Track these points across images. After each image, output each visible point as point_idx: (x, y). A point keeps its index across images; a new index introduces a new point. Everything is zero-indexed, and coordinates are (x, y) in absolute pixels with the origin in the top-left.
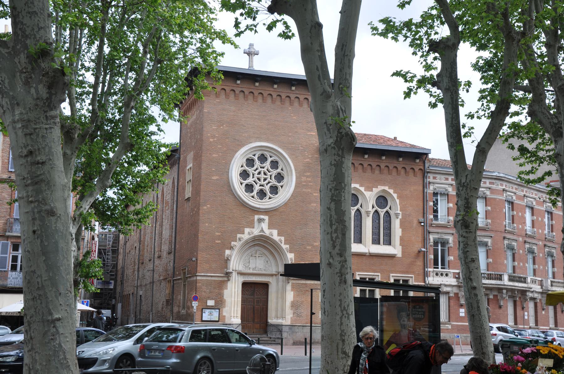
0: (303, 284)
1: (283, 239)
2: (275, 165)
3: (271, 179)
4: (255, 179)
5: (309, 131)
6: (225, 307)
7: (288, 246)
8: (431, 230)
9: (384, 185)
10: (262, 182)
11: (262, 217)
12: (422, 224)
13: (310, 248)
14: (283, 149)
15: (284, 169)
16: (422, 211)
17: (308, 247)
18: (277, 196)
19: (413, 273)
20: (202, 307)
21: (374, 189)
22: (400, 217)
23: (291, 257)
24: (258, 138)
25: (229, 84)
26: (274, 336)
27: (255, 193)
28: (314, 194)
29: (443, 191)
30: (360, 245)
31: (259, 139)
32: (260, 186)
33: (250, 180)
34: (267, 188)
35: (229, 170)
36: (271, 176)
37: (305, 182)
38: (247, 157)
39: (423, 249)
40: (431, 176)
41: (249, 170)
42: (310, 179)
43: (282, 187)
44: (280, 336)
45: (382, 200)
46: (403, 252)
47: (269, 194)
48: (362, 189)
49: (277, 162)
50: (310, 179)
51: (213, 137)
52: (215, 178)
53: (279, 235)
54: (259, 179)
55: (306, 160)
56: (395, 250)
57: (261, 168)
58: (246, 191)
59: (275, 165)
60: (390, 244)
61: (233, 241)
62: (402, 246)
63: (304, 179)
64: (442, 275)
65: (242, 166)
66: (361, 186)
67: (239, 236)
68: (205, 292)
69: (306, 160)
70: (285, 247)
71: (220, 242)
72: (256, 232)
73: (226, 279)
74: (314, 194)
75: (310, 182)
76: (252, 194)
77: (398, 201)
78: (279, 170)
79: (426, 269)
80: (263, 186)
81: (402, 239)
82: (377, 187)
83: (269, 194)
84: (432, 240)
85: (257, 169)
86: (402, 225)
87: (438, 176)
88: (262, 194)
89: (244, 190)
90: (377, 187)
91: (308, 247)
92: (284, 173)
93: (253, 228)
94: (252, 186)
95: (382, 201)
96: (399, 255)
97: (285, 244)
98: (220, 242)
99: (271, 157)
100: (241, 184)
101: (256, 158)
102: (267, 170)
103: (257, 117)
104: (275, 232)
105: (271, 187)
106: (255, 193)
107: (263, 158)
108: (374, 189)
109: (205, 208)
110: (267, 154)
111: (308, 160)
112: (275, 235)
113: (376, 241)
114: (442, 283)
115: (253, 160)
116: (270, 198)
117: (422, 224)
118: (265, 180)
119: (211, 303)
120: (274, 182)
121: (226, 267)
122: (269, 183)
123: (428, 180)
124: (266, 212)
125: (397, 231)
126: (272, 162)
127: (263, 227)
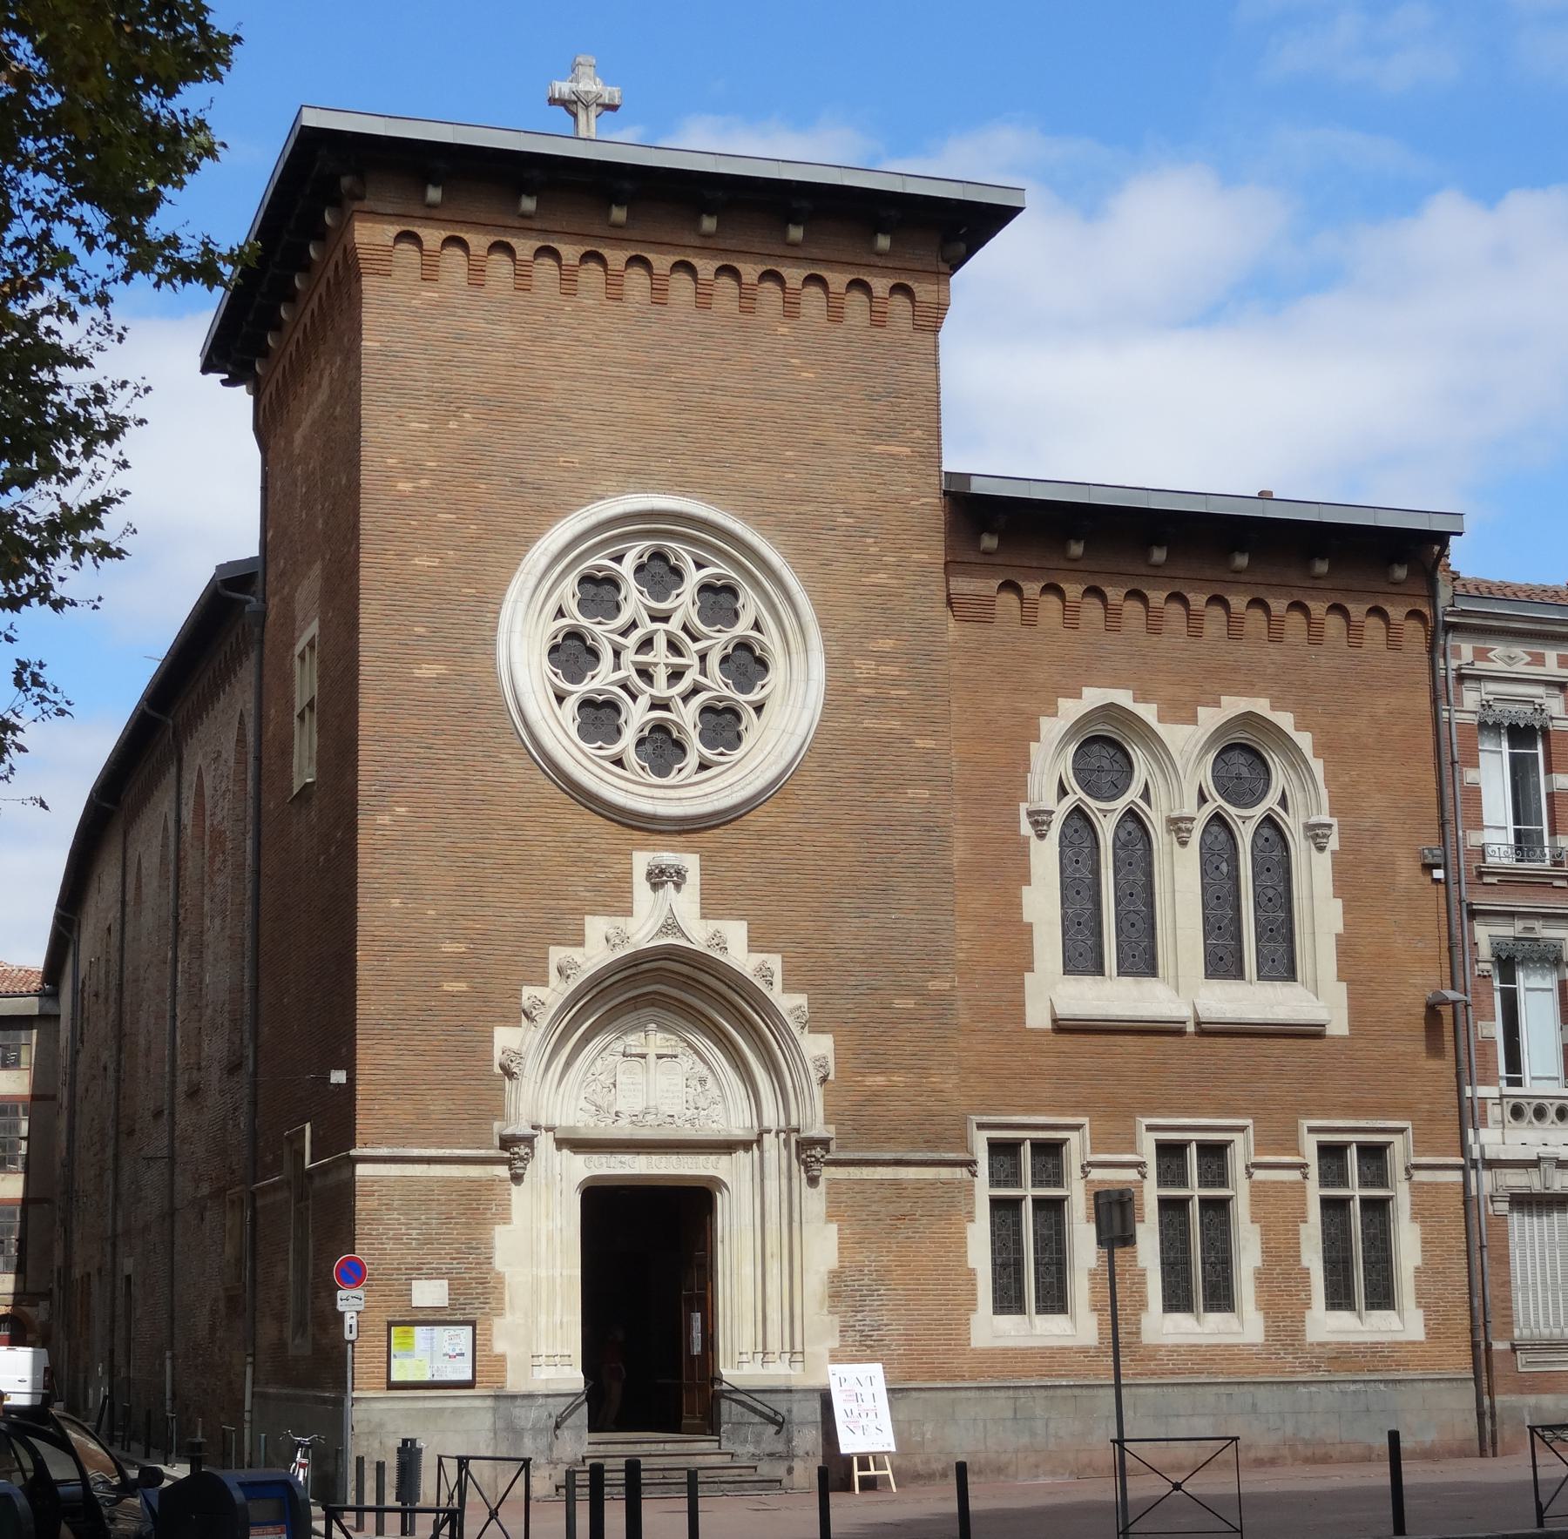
0: (881, 1183)
1: (775, 962)
2: (719, 599)
3: (703, 672)
5: (879, 437)
7: (801, 1000)
8: (1482, 901)
9: (1249, 690)
10: (661, 689)
11: (668, 858)
12: (1439, 874)
13: (910, 1003)
14: (759, 527)
15: (768, 622)
16: (1434, 811)
17: (899, 1003)
18: (737, 754)
19: (1405, 1110)
20: (385, 1317)
21: (1202, 712)
22: (1333, 843)
23: (817, 1052)
25: (483, 218)
26: (751, 1448)
27: (629, 738)
28: (919, 743)
29: (1522, 714)
30: (1147, 983)
31: (639, 479)
32: (653, 707)
33: (602, 679)
34: (687, 717)
35: (495, 629)
36: (703, 658)
37: (868, 683)
39: (1452, 995)
41: (598, 629)
43: (759, 709)
44: (780, 1447)
47: (696, 749)
48: (1147, 712)
49: (731, 591)
50: (894, 671)
51: (413, 470)
52: (427, 671)
54: (645, 673)
55: (874, 579)
56: (1316, 998)
57: (653, 619)
58: (586, 733)
59: (719, 599)
60: (1290, 974)
61: (531, 983)
62: (1350, 982)
63: (865, 668)
64: (1540, 1113)
65: (560, 613)
67: (557, 954)
69: (874, 579)
70: (788, 1003)
71: (462, 986)
73: (503, 1171)
74: (919, 743)
75: (896, 683)
76: (614, 750)
77: (1317, 766)
78: (742, 628)
79: (1468, 1091)
80: (666, 707)
81: (1346, 949)
82: (1217, 704)
83: (696, 749)
84: (1485, 951)
85: (634, 625)
86: (1345, 883)
87: (1499, 650)
88: (662, 746)
89: (573, 730)
90: (1217, 704)
91: (899, 1003)
92: (771, 641)
93: (629, 913)
94: (612, 706)
95: (1245, 772)
96: (1339, 1026)
97: (788, 988)
98: (462, 986)
99: (699, 566)
100: (560, 699)
101: (626, 569)
102: (685, 628)
103: (624, 372)
105: (706, 710)
106: (629, 738)
107: (660, 573)
108: (1202, 712)
109: (385, 819)
110: (683, 554)
111: (881, 578)
112: (733, 945)
113: (1222, 962)
114: (1544, 1152)
115: (613, 582)
116: (703, 767)
117: (1439, 874)
118: (676, 675)
119: (429, 1293)
120: (718, 686)
121: (498, 1112)
122: (696, 690)
123: (1454, 664)
126: (705, 588)
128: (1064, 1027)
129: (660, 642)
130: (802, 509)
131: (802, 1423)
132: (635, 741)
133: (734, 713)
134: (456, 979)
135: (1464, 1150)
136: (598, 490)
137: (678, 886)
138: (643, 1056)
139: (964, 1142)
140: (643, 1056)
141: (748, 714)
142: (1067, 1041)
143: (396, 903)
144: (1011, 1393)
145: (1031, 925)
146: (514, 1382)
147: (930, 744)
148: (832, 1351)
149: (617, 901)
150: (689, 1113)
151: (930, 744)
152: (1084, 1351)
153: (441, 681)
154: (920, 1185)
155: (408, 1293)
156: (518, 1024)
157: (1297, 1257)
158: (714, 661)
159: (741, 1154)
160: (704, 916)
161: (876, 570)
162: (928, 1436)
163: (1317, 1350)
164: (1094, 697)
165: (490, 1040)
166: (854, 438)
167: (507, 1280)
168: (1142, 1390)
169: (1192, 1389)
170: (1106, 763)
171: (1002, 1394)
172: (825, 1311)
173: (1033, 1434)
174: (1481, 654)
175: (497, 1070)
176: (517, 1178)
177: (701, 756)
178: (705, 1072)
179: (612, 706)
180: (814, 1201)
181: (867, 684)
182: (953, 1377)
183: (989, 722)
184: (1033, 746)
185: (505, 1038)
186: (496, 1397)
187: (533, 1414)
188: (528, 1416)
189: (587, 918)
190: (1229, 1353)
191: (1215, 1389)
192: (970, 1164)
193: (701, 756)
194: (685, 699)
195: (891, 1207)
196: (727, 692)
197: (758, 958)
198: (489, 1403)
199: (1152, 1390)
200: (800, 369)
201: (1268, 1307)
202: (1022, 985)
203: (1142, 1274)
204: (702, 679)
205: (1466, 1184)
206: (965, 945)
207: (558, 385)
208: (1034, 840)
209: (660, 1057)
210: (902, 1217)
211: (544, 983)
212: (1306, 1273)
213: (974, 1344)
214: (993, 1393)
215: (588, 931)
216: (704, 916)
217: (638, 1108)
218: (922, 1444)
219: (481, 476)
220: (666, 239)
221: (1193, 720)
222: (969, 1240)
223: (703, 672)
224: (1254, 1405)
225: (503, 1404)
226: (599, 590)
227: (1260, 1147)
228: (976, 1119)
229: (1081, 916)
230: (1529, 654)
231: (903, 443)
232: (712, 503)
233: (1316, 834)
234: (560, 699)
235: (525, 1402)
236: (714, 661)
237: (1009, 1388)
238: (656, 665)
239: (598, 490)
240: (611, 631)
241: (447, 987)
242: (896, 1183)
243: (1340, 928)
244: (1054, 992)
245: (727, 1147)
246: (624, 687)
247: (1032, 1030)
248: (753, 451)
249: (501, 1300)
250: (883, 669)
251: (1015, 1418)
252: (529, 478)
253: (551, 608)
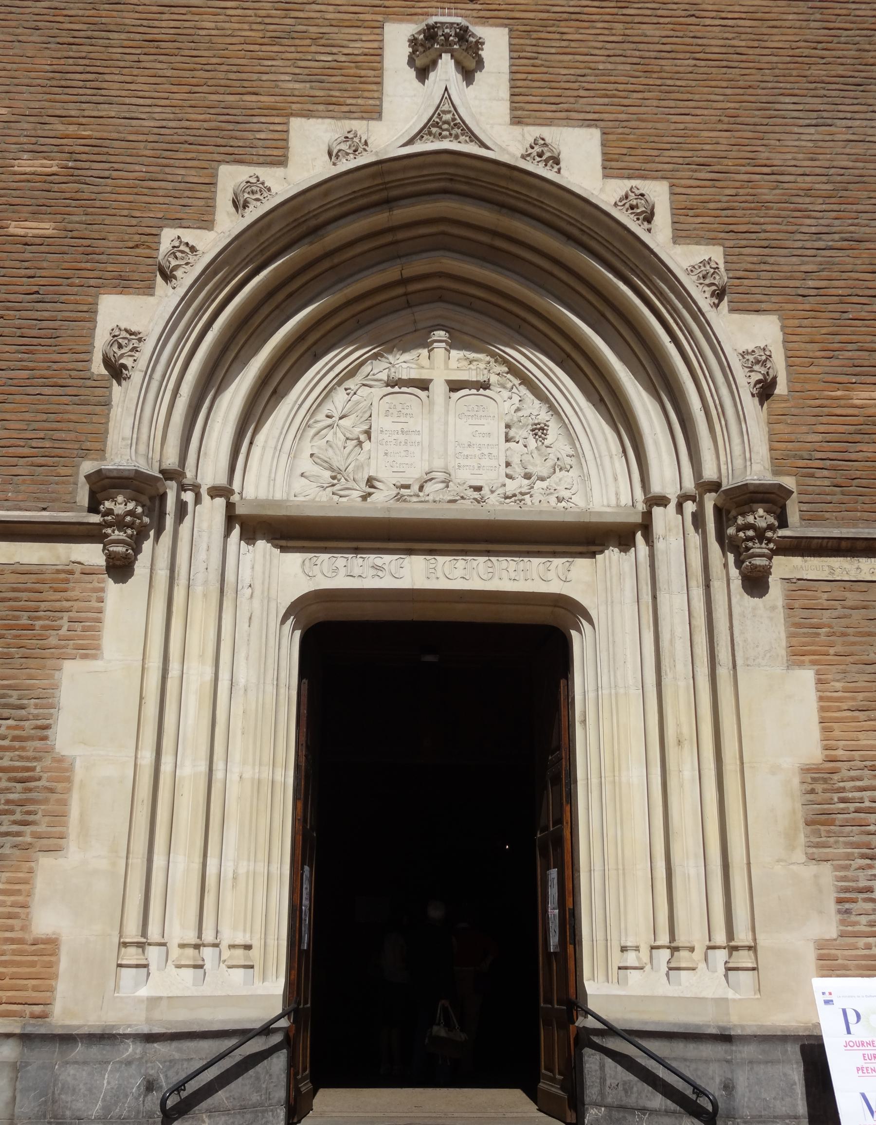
6: (54, 843)
53: (612, 165)
61: (178, 222)
67: (231, 177)
71: (46, 228)
73: (92, 554)
93: (375, 113)
97: (681, 234)
98: (46, 228)
121: (96, 441)
134: (35, 215)
137: (468, 75)
138: (424, 385)
146: (73, 1005)
148: (821, 945)
149: (354, 91)
156: (149, 290)
159: (612, 555)
160: (516, 121)
165: (92, 313)
167: (79, 773)
172: (799, 856)
175: (98, 368)
178: (543, 415)
180: (761, 623)
185: (115, 311)
186: (25, 1038)
187: (107, 1081)
189: (295, 123)
209: (455, 386)
211: (206, 223)
215: (295, 142)
216: (516, 121)
217: (413, 475)
225: (41, 1055)
235: (95, 1051)
241: (14, 228)
245: (585, 539)
249: (60, 816)
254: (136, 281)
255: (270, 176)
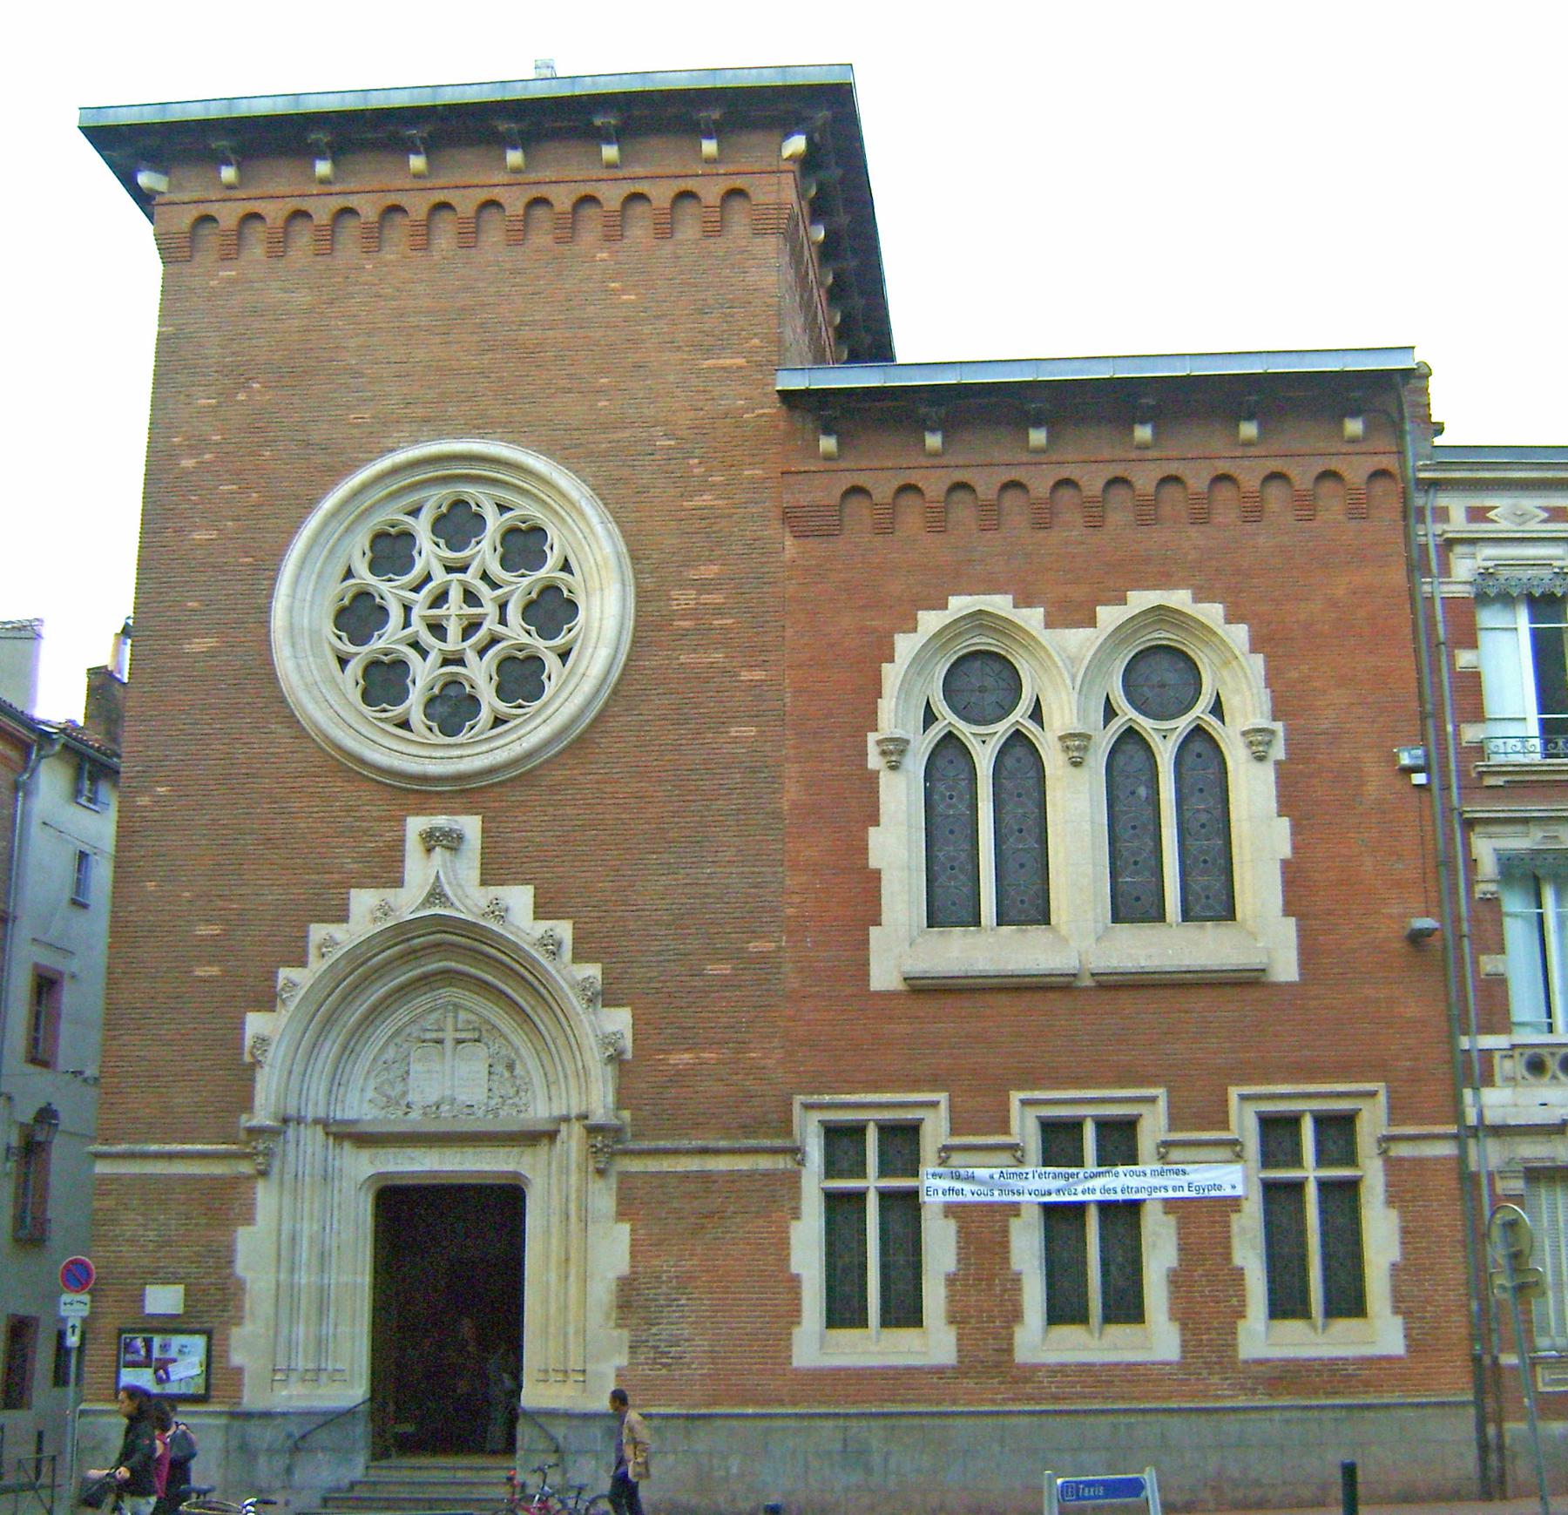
0: (686, 1176)
1: (564, 930)
4: (418, 627)
5: (708, 352)
6: (239, 1321)
8: (1477, 809)
9: (1165, 581)
10: (453, 643)
11: (441, 821)
12: (1419, 778)
13: (725, 969)
17: (711, 969)
20: (117, 1323)
21: (1102, 612)
22: (1278, 751)
24: (426, 420)
28: (745, 675)
30: (1035, 933)
32: (446, 662)
35: (270, 596)
36: (503, 607)
38: (378, 520)
40: (1457, 506)
42: (718, 598)
43: (564, 656)
45: (1161, 671)
46: (1308, 952)
50: (718, 598)
52: (199, 645)
54: (437, 629)
55: (697, 501)
61: (289, 964)
63: (683, 599)
66: (1024, 600)
67: (318, 932)
68: (132, 1241)
69: (697, 501)
71: (214, 970)
72: (407, 902)
74: (745, 675)
75: (719, 611)
80: (461, 662)
81: (1294, 877)
85: (428, 578)
86: (1290, 798)
89: (355, 695)
91: (711, 969)
93: (399, 883)
96: (1286, 969)
98: (214, 970)
99: (503, 508)
100: (343, 662)
102: (485, 577)
104: (519, 898)
107: (458, 525)
108: (1102, 612)
110: (482, 498)
111: (707, 499)
113: (1133, 903)
115: (408, 536)
116: (498, 721)
118: (471, 628)
119: (164, 1299)
122: (494, 640)
124: (462, 791)
125: (1260, 834)
127: (437, 873)
128: (923, 989)
129: (455, 595)
130: (620, 435)
131: (579, 1452)
132: (424, 700)
133: (536, 661)
134: (209, 963)
135: (1458, 1115)
136: (389, 443)
138: (440, 1042)
139: (785, 1126)
140: (440, 1042)
141: (551, 661)
142: (930, 1007)
143: (151, 886)
144: (841, 1422)
145: (878, 872)
146: (252, 1399)
147: (758, 675)
149: (389, 872)
150: (493, 1103)
151: (758, 675)
152: (939, 1371)
153: (212, 653)
154: (733, 1177)
155: (140, 1299)
157: (1227, 1256)
158: (514, 613)
160: (483, 883)
161: (701, 492)
162: (734, 1470)
163: (1254, 1368)
164: (960, 604)
165: (241, 1027)
166: (679, 355)
168: (1013, 1420)
169: (1081, 1419)
170: (989, 682)
171: (830, 1423)
172: (612, 1324)
173: (868, 1470)
174: (1477, 514)
176: (263, 1174)
177: (493, 710)
179: (401, 665)
181: (683, 618)
182: (768, 1402)
183: (831, 645)
184: (886, 667)
185: (256, 1023)
186: (233, 1415)
187: (269, 1434)
188: (263, 1435)
189: (353, 892)
190: (1133, 1374)
191: (1111, 1419)
192: (796, 1152)
193: (493, 710)
194: (482, 653)
195: (696, 1203)
196: (525, 639)
197: (543, 926)
198: (223, 1421)
199: (1025, 1420)
200: (624, 291)
201: (1185, 1315)
202: (867, 941)
203: (1017, 1279)
204: (500, 629)
205: (1462, 1158)
206: (796, 899)
207: (352, 343)
208: (886, 779)
209: (459, 1042)
210: (710, 1215)
211: (303, 964)
212: (1238, 1275)
213: (796, 1363)
214: (818, 1422)
216: (483, 883)
217: (434, 1098)
218: (726, 1479)
219: (267, 443)
220: (476, 181)
221: (1091, 622)
222: (792, 1242)
223: (503, 621)
224: (1163, 1436)
225: (236, 1423)
226: (391, 551)
227: (1175, 1122)
228: (799, 1099)
229: (954, 859)
230: (1545, 509)
231: (738, 354)
232: (513, 442)
233: (1257, 741)
234: (343, 662)
236: (514, 613)
237: (837, 1415)
238: (448, 617)
239: (389, 443)
240: (401, 587)
242: (705, 1177)
243: (1286, 851)
244: (901, 947)
246: (415, 645)
247: (878, 994)
248: (563, 383)
249: (240, 1308)
250: (705, 598)
251: (844, 1451)
252: (315, 437)
253: (340, 571)
254: (268, 1001)
255: (337, 931)
